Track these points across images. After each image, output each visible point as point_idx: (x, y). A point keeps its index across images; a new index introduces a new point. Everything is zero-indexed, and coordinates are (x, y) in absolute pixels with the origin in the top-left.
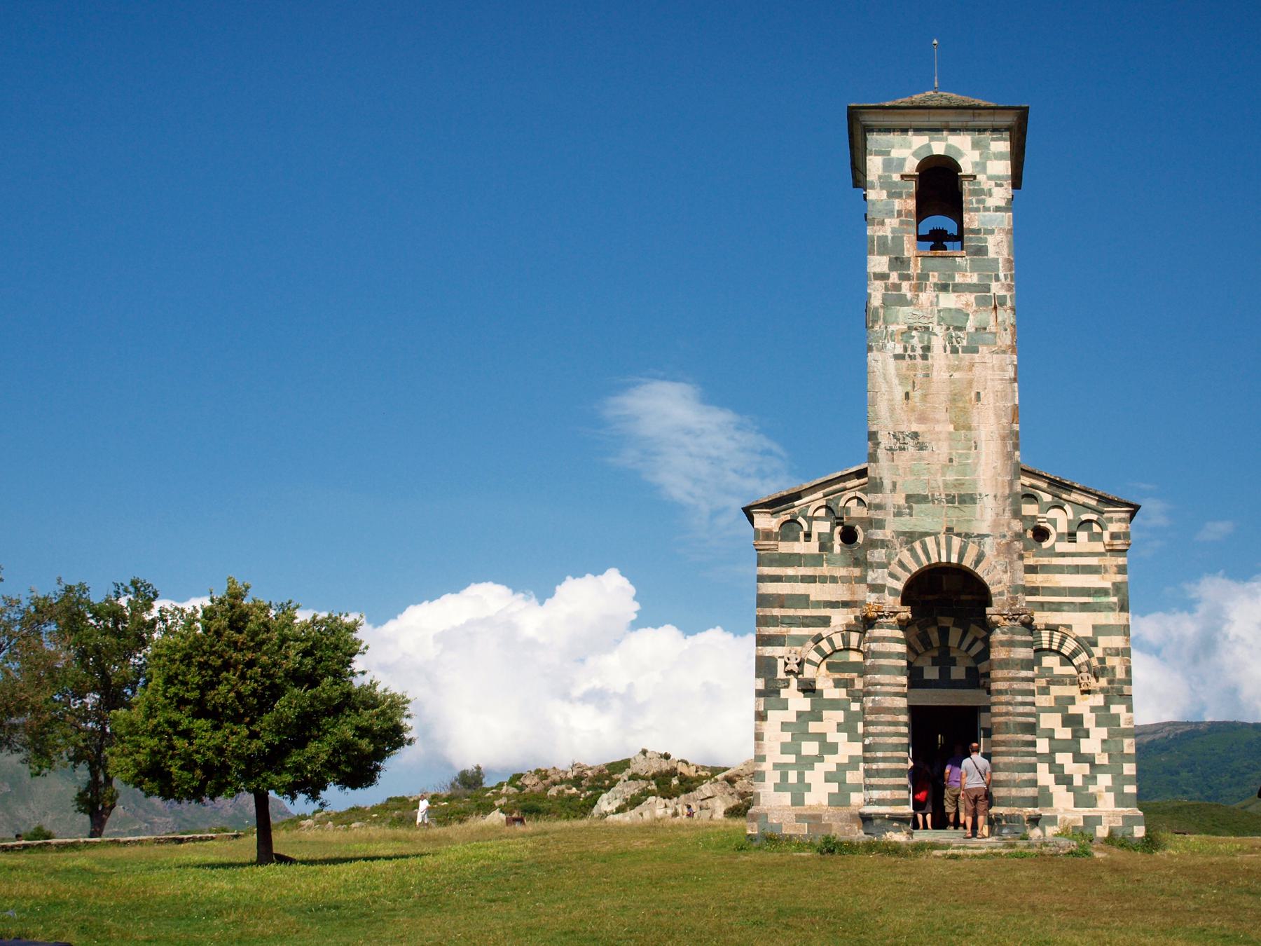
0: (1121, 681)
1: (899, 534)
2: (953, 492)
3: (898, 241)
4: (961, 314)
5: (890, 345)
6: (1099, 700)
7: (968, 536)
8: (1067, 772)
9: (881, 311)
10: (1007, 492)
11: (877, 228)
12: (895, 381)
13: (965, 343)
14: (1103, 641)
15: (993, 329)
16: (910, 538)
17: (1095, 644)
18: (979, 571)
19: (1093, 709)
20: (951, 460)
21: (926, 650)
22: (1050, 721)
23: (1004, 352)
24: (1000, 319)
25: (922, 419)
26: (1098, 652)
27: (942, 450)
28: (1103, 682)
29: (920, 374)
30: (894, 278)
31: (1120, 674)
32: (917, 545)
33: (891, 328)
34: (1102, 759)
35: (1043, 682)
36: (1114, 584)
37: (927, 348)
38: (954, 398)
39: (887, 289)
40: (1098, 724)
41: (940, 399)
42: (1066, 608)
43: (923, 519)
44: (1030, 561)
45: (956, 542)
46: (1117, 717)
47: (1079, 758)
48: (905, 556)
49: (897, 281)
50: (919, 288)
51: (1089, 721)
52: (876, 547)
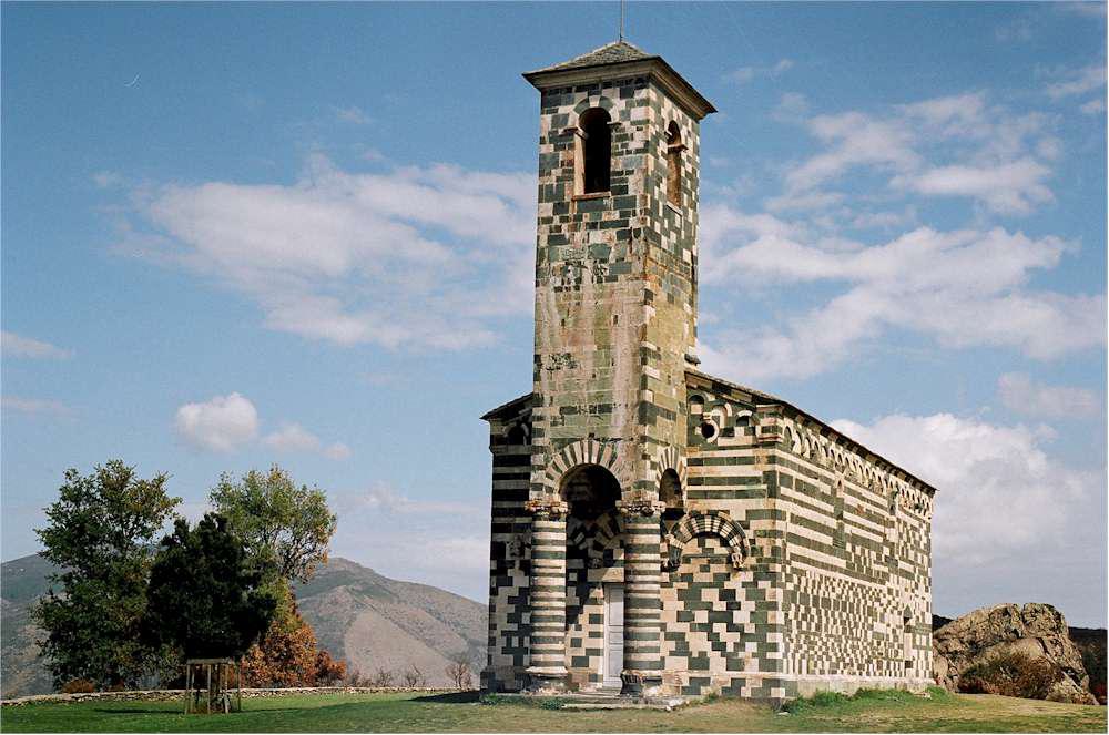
0: (768, 560)
1: (555, 440)
2: (596, 403)
3: (561, 188)
4: (605, 248)
5: (552, 279)
6: (749, 576)
7: (605, 440)
9: (546, 251)
10: (636, 400)
11: (546, 178)
12: (555, 310)
13: (607, 273)
14: (754, 524)
15: (629, 260)
16: (563, 443)
17: (747, 528)
18: (611, 470)
19: (744, 585)
20: (594, 376)
21: (615, 535)
22: (710, 595)
23: (637, 279)
24: (634, 250)
25: (574, 342)
26: (749, 534)
27: (587, 368)
28: (752, 561)
29: (574, 302)
30: (557, 218)
31: (767, 554)
32: (567, 449)
33: (553, 265)
34: (750, 629)
35: (704, 561)
36: (764, 473)
37: (579, 280)
38: (598, 322)
39: (551, 232)
41: (588, 325)
42: (724, 495)
43: (576, 427)
44: (698, 455)
45: (596, 445)
47: (732, 627)
48: (558, 459)
49: (559, 224)
50: (575, 228)
51: (741, 596)
52: (537, 453)
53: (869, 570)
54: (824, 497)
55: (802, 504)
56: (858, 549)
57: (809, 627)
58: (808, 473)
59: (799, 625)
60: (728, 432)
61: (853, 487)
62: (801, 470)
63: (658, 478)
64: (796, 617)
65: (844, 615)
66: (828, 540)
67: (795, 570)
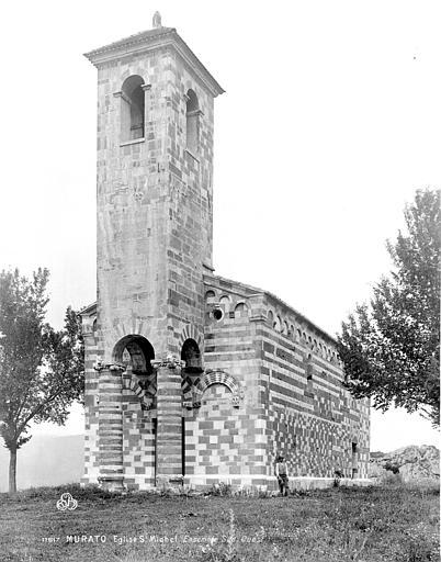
8: (226, 455)
40: (243, 427)
46: (253, 421)
51: (238, 425)
53: (330, 412)
54: (297, 363)
55: (281, 365)
56: (323, 399)
57: (286, 445)
58: (287, 346)
59: (279, 444)
60: (232, 315)
61: (320, 360)
62: (281, 342)
64: (276, 439)
65: (312, 440)
66: (302, 392)
67: (276, 409)
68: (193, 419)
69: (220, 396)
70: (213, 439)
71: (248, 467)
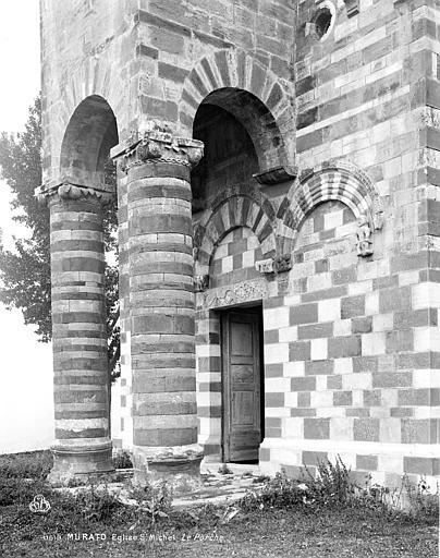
8: (346, 387)
19: (378, 284)
40: (383, 311)
51: (372, 304)
63: (186, 97)
68: (278, 302)
69: (332, 232)
70: (319, 349)
71: (396, 421)
